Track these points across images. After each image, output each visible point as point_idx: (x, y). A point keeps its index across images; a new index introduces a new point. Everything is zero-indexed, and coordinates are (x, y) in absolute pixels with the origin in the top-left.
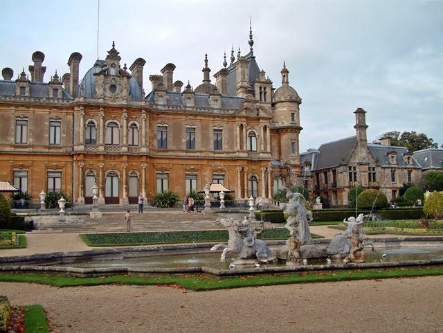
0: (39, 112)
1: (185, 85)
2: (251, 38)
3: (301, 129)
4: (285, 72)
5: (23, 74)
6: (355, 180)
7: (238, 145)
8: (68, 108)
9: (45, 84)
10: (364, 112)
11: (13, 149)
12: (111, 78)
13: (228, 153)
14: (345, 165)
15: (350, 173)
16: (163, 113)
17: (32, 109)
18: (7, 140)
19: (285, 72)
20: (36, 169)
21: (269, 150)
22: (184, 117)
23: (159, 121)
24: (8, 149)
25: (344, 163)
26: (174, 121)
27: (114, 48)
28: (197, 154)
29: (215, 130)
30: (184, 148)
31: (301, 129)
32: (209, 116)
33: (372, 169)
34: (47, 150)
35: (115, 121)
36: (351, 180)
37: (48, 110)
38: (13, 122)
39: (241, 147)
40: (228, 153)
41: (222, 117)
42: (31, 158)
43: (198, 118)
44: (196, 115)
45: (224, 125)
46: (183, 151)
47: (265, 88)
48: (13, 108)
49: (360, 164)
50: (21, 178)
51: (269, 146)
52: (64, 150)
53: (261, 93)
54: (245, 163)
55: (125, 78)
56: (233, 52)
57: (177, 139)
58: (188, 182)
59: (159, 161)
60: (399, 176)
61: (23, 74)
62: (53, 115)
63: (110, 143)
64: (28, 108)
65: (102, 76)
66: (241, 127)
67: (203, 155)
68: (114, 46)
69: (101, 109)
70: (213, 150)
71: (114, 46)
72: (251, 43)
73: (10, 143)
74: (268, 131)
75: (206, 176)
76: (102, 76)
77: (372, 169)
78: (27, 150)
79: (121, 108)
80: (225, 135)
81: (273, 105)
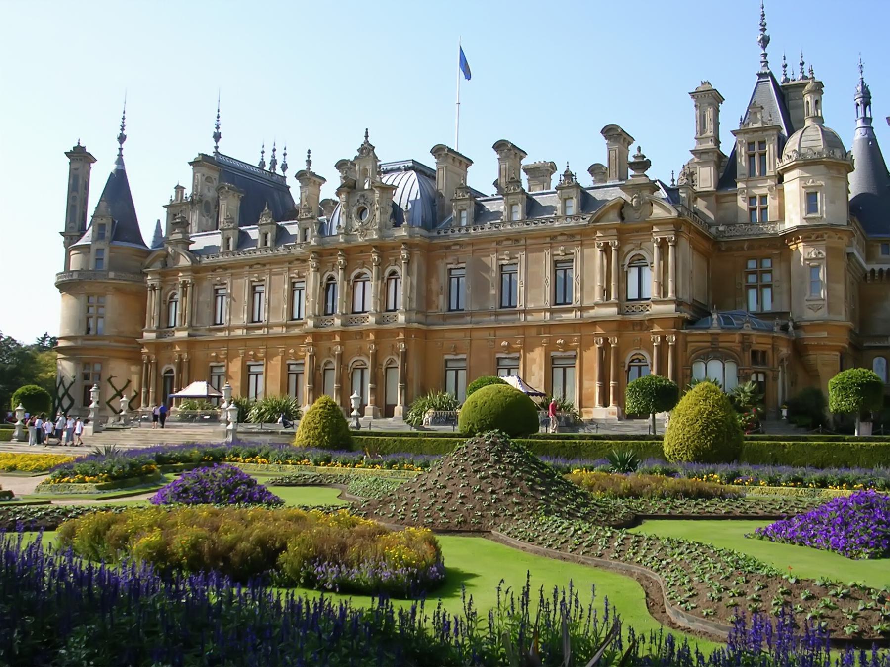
1: (561, 170)
12: (360, 193)
16: (456, 244)
17: (268, 266)
23: (450, 260)
27: (367, 142)
39: (606, 292)
47: (762, 144)
50: (219, 376)
53: (751, 157)
59: (447, 335)
60: (565, 351)
63: (361, 310)
64: (264, 265)
66: (606, 249)
68: (367, 137)
71: (367, 137)
81: (781, 180)
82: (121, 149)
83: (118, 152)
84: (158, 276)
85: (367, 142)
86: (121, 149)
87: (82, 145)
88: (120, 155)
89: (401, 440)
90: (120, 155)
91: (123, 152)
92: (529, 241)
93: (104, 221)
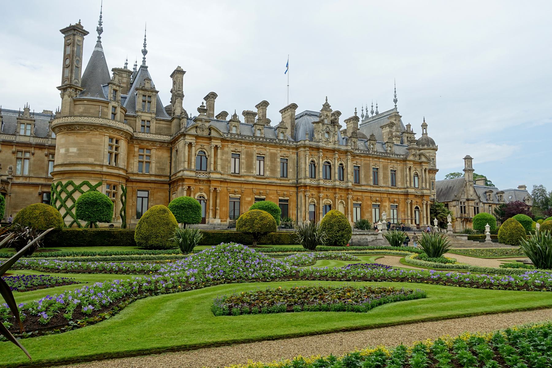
0: (273, 150)
2: (395, 97)
3: (437, 170)
4: (424, 126)
5: (235, 115)
6: (465, 213)
7: (408, 183)
8: (293, 148)
9: (271, 128)
10: (471, 159)
11: (255, 179)
13: (400, 188)
14: (458, 201)
15: (461, 207)
16: (357, 156)
17: (267, 148)
18: (250, 172)
19: (424, 126)
20: (271, 196)
21: (428, 187)
22: (371, 159)
24: (251, 179)
25: (456, 198)
26: (365, 162)
27: (327, 102)
28: (381, 189)
29: (391, 170)
30: (372, 183)
31: (437, 170)
32: (388, 160)
33: (463, 203)
34: (279, 182)
35: (329, 161)
36: (462, 212)
37: (279, 149)
38: (255, 158)
40: (400, 188)
41: (397, 161)
42: (268, 188)
43: (381, 160)
44: (379, 158)
45: (398, 167)
46: (371, 186)
48: (255, 146)
49: (468, 200)
51: (428, 184)
52: (291, 181)
54: (413, 196)
55: (336, 126)
56: (372, 106)
57: (367, 177)
58: (373, 210)
61: (235, 115)
62: (282, 153)
64: (266, 146)
65: (321, 124)
67: (384, 189)
68: (327, 100)
69: (321, 150)
70: (390, 185)
71: (327, 100)
72: (395, 101)
73: (252, 174)
74: (427, 172)
75: (386, 206)
76: (321, 124)
77: (463, 203)
78: (264, 181)
79: (334, 151)
80: (399, 175)
82: (99, 38)
83: (97, 39)
84: (194, 139)
85: (327, 102)
86: (99, 38)
87: (82, 24)
88: (99, 41)
89: (41, 231)
90: (99, 41)
91: (101, 40)
92: (383, 160)
93: (117, 88)
